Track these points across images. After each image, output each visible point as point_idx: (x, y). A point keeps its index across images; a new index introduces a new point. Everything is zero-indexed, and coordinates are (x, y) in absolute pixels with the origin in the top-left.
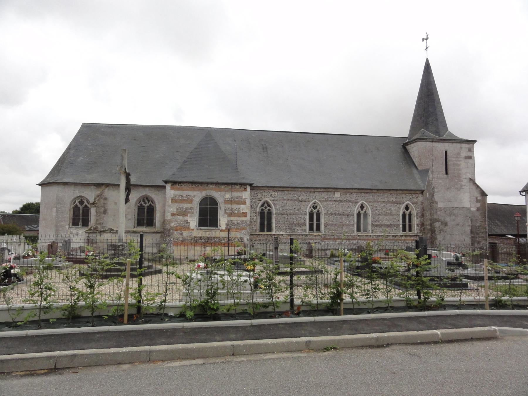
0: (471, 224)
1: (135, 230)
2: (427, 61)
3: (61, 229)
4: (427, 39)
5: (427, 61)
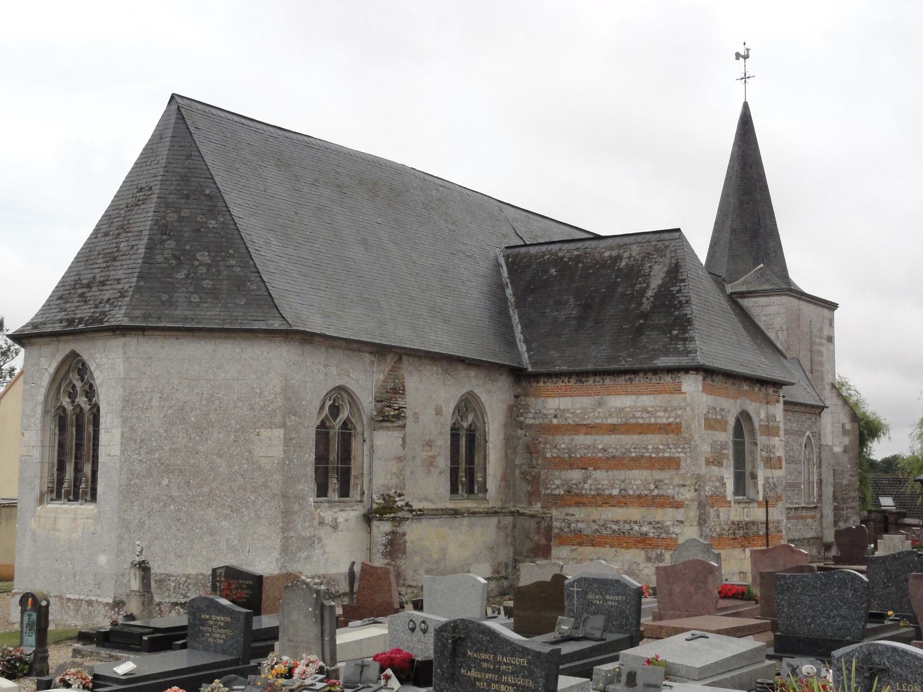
0: (834, 480)
1: (451, 505)
2: (746, 106)
3: (296, 507)
4: (746, 57)
5: (746, 106)
